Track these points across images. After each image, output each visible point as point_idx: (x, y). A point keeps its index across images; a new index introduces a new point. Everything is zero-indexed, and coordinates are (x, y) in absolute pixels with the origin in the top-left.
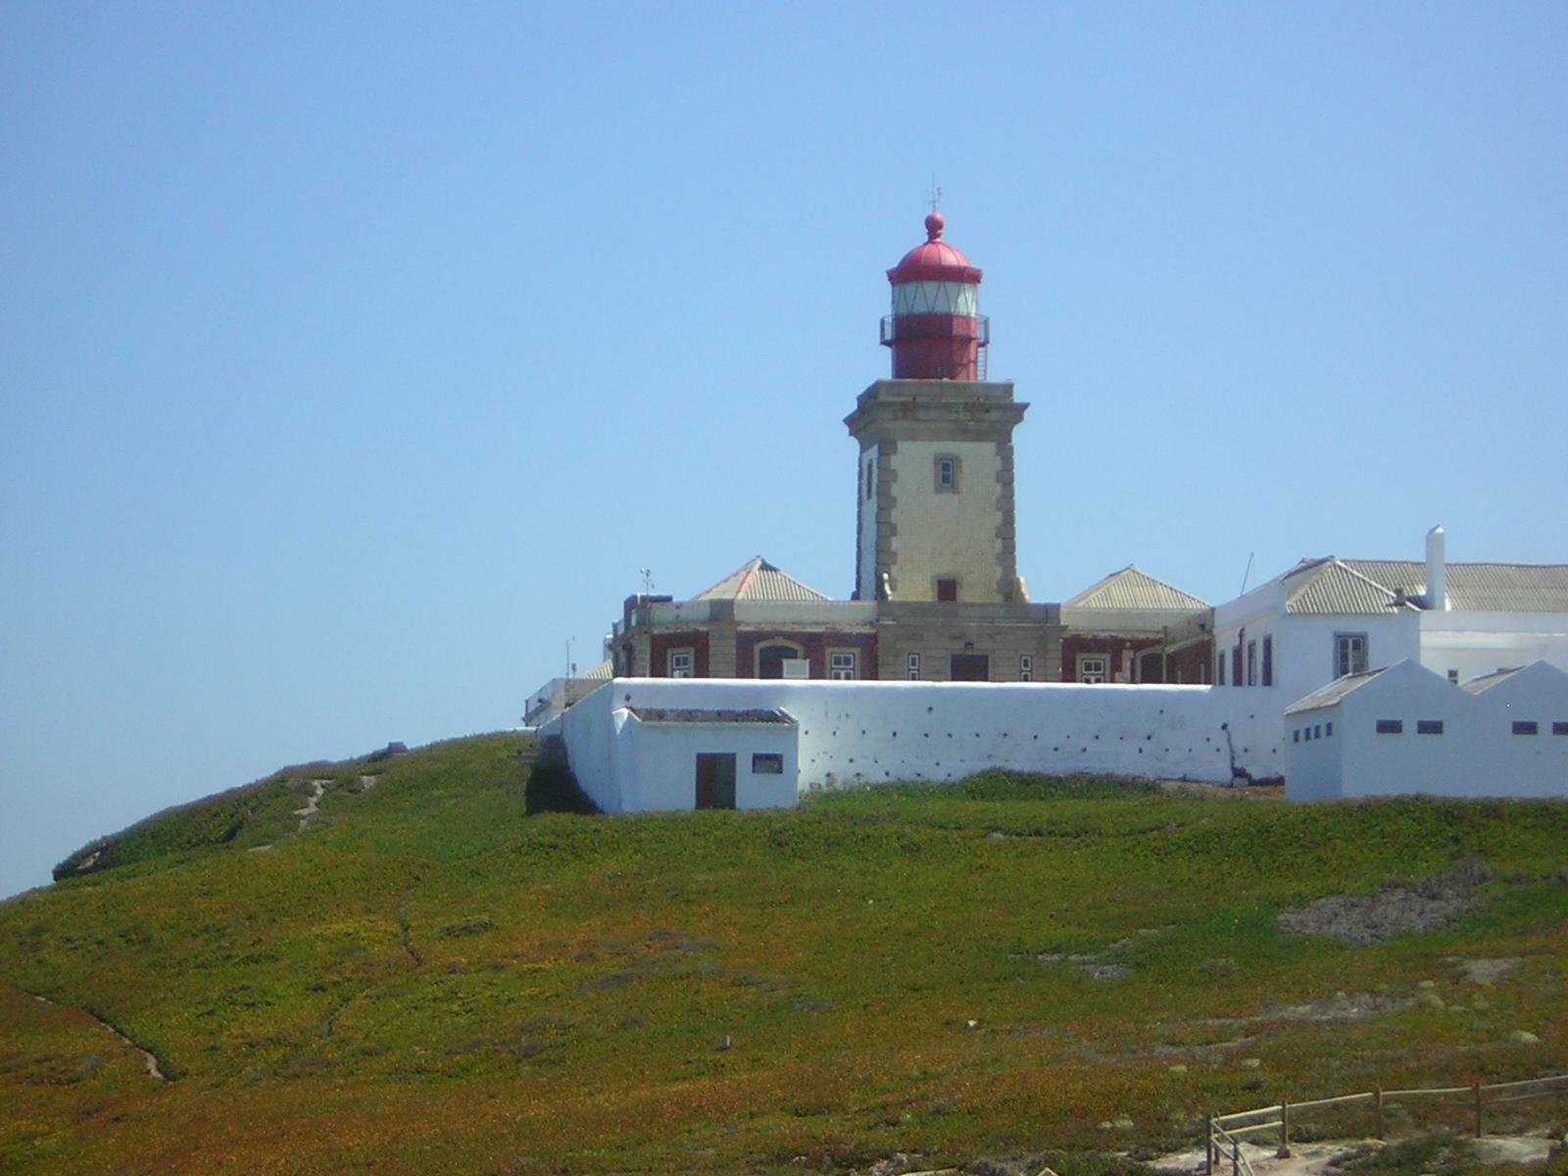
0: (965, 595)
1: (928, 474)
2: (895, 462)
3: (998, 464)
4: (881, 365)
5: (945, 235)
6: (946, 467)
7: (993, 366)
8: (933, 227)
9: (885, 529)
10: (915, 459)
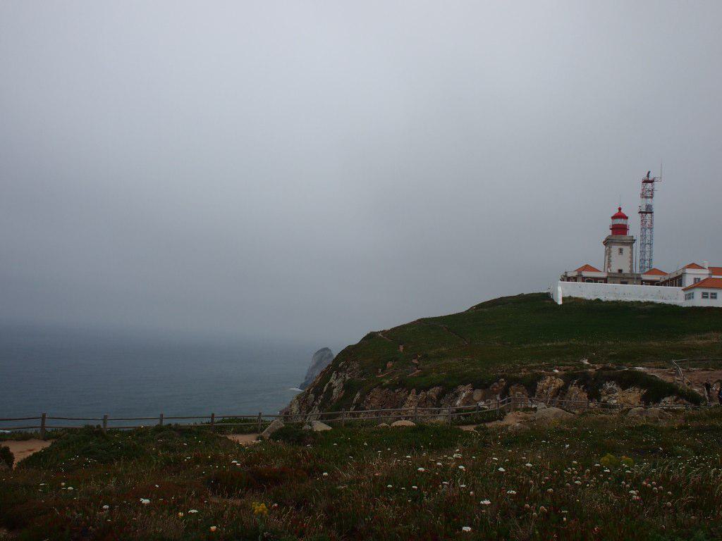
0: (624, 272)
1: (617, 252)
2: (612, 249)
3: (630, 250)
4: (610, 233)
5: (622, 211)
6: (621, 251)
7: (631, 233)
8: (620, 209)
9: (610, 261)
10: (615, 249)
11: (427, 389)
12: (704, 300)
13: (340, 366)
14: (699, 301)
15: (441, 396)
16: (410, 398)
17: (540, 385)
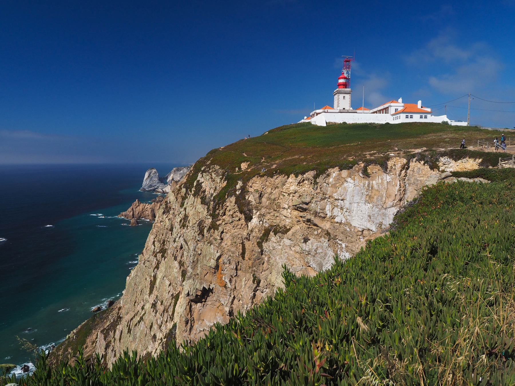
10: (341, 96)
11: (303, 173)
12: (407, 119)
13: (202, 169)
14: (402, 119)
15: (316, 177)
16: (290, 180)
17: (390, 163)
